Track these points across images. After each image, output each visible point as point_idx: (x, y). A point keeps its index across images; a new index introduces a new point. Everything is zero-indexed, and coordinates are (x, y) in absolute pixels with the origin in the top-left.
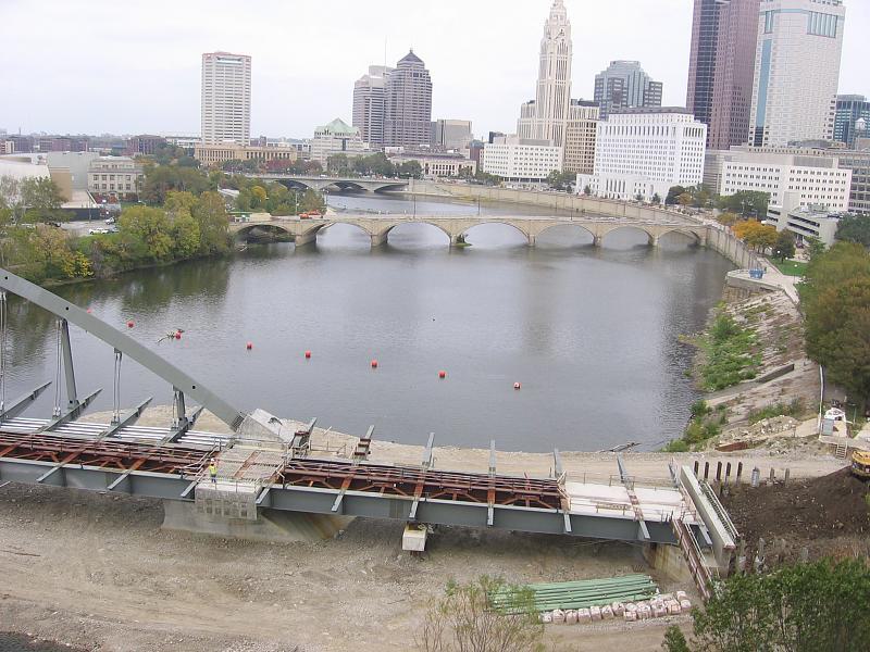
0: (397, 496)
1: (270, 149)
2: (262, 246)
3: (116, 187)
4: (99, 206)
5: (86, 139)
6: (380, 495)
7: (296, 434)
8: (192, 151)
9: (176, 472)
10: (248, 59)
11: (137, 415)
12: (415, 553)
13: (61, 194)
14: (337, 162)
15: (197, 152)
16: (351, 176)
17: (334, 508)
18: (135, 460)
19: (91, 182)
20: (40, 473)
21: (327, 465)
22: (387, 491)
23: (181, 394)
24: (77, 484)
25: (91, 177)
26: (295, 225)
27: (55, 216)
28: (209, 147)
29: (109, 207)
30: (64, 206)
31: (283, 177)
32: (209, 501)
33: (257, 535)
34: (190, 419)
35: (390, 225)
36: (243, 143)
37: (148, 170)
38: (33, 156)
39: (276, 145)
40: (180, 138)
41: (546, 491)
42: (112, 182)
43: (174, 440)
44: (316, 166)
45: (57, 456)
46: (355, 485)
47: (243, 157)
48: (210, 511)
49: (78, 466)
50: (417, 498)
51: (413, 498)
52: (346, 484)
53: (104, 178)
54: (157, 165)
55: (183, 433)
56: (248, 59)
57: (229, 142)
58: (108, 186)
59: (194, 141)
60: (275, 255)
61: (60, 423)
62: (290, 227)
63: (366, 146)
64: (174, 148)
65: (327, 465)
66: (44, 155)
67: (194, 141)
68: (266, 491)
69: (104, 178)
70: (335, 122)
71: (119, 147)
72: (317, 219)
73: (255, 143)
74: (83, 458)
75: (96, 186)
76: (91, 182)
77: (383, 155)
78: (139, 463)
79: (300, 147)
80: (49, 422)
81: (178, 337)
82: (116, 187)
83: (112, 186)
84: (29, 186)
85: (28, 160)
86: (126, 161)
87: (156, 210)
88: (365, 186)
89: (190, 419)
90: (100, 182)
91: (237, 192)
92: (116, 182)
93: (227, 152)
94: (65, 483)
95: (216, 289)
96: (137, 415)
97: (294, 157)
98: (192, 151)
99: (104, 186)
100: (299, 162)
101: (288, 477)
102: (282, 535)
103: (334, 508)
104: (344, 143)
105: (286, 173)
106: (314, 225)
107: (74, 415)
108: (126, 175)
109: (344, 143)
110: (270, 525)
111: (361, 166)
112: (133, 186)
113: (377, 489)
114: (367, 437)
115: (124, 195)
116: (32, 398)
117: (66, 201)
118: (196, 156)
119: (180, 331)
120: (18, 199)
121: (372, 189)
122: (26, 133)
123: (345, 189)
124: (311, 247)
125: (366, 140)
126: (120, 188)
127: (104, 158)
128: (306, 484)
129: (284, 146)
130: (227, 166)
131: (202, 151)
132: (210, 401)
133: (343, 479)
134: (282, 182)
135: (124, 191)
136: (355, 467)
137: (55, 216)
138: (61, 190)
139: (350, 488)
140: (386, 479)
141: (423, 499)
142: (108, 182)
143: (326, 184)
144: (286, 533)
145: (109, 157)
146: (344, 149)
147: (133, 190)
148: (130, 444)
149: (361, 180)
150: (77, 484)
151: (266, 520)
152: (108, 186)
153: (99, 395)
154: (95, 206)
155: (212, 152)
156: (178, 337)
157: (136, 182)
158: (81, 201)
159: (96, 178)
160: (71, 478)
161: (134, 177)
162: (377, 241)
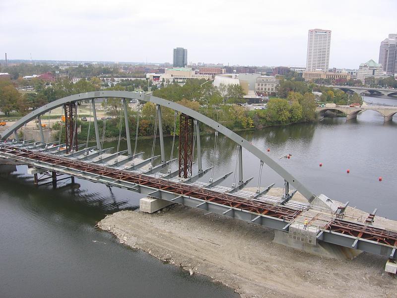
1: (338, 74)
2: (331, 119)
3: (267, 89)
4: (259, 97)
5: (255, 68)
6: (376, 243)
7: (339, 208)
8: (301, 74)
9: (282, 218)
10: (330, 32)
11: (267, 190)
12: (391, 274)
13: (244, 92)
14: (369, 80)
15: (304, 75)
16: (376, 87)
17: (353, 246)
18: (264, 210)
19: (257, 87)
20: (224, 210)
22: (380, 241)
23: (288, 183)
24: (239, 217)
25: (257, 84)
27: (240, 101)
28: (309, 72)
29: (263, 98)
31: (343, 87)
32: (295, 233)
33: (314, 252)
34: (291, 195)
35: (394, 112)
36: (325, 71)
37: (281, 82)
38: (233, 75)
39: (341, 72)
40: (297, 68)
42: (266, 87)
43: (283, 204)
44: (359, 82)
45: (206, 198)
46: (364, 236)
47: (324, 77)
48: (295, 238)
51: (393, 247)
52: (360, 235)
53: (262, 86)
54: (285, 80)
55: (287, 201)
56: (330, 32)
57: (318, 70)
58: (264, 89)
59: (302, 69)
60: (337, 123)
61: (234, 190)
62: (344, 111)
63: (385, 73)
64: (293, 72)
66: (238, 75)
67: (302, 69)
68: (322, 232)
69: (262, 86)
70: (370, 61)
71: (269, 72)
72: (358, 107)
73: (330, 71)
74: (242, 206)
75: (259, 89)
76: (257, 87)
77: (393, 78)
78: (266, 212)
79: (352, 73)
80: (230, 189)
81: (289, 158)
82: (267, 89)
84: (231, 88)
85: (231, 77)
86: (272, 78)
87: (284, 100)
88: (383, 92)
89: (291, 195)
90: (260, 87)
91: (321, 93)
92: (267, 87)
93: (317, 75)
94: (234, 216)
95: (307, 137)
96: (267, 190)
97: (349, 78)
98: (301, 74)
99: (262, 89)
100: (351, 80)
101: (332, 228)
102: (327, 254)
103: (353, 246)
104: (374, 71)
107: (241, 187)
108: (272, 84)
109: (374, 71)
110: (322, 249)
111: (382, 83)
113: (375, 240)
114: (373, 214)
115: (270, 93)
116: (224, 178)
117: (245, 95)
118: (303, 77)
119: (290, 155)
120: (226, 93)
121: (386, 94)
122: (231, 65)
123: (373, 94)
124: (354, 120)
125: (385, 70)
127: (263, 76)
128: (341, 232)
129: (344, 72)
130: (317, 81)
131: (306, 74)
132: (300, 188)
133: (359, 232)
134: (343, 89)
135: (270, 91)
136: (366, 228)
137: (240, 101)
138: (243, 89)
139: (362, 237)
140: (381, 236)
142: (264, 87)
143: (364, 91)
144: (328, 253)
145: (265, 76)
146: (373, 74)
147: (274, 91)
148: (263, 203)
149: (382, 90)
150: (239, 217)
151: (320, 246)
152: (264, 89)
153: (252, 180)
154: (257, 97)
155: (310, 74)
156: (289, 158)
157: (276, 87)
158: (252, 95)
159: (259, 85)
160: (236, 214)
161: (275, 85)
162: (387, 119)
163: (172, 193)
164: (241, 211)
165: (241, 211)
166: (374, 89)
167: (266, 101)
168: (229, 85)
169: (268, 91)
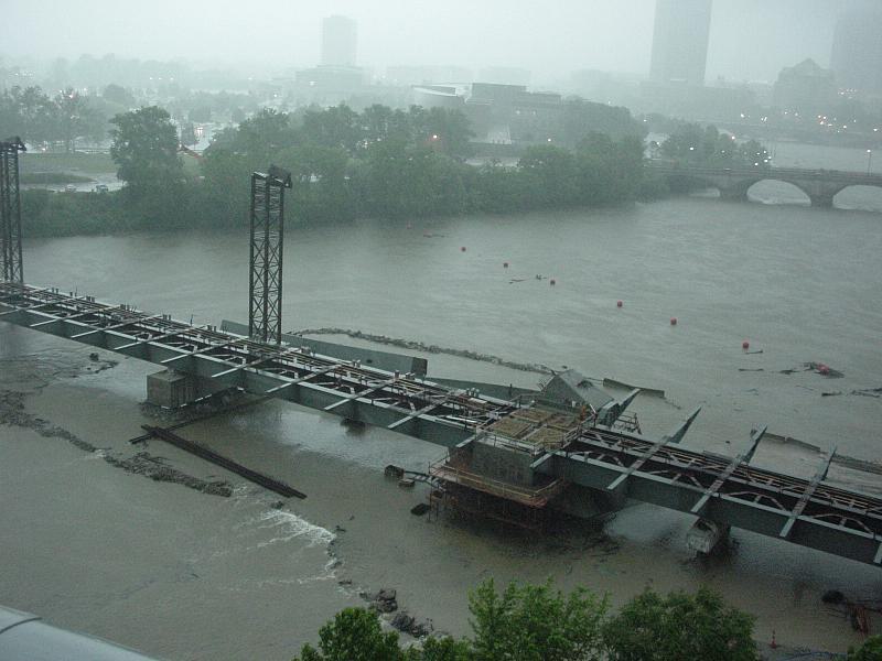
0: (689, 486)
17: (611, 487)
18: (429, 403)
21: (627, 440)
22: (683, 479)
41: (873, 512)
46: (649, 466)
49: (369, 401)
50: (711, 492)
65: (631, 442)
68: (547, 456)
74: (378, 393)
78: (431, 407)
101: (576, 446)
103: (611, 487)
113: (671, 476)
128: (593, 456)
133: (637, 458)
141: (716, 495)
163: (220, 361)
164: (372, 404)
165: (372, 404)
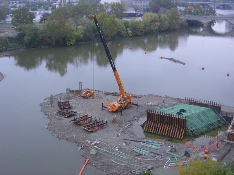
4: (136, 12)
16: (227, 2)
26: (205, 21)
27: (121, 15)
29: (139, 13)
30: (124, 12)
62: (202, 21)
75: (136, 5)
82: (143, 5)
83: (141, 5)
105: (203, 1)
106: (213, 20)
112: (148, 5)
115: (145, 9)
117: (125, 10)
120: (109, 10)
126: (144, 6)
135: (145, 7)
137: (121, 15)
152: (140, 6)
154: (135, 12)
157: (150, 4)
158: (131, 11)
166: (226, 3)
167: (141, 15)
168: (112, 3)
169: (144, 7)
